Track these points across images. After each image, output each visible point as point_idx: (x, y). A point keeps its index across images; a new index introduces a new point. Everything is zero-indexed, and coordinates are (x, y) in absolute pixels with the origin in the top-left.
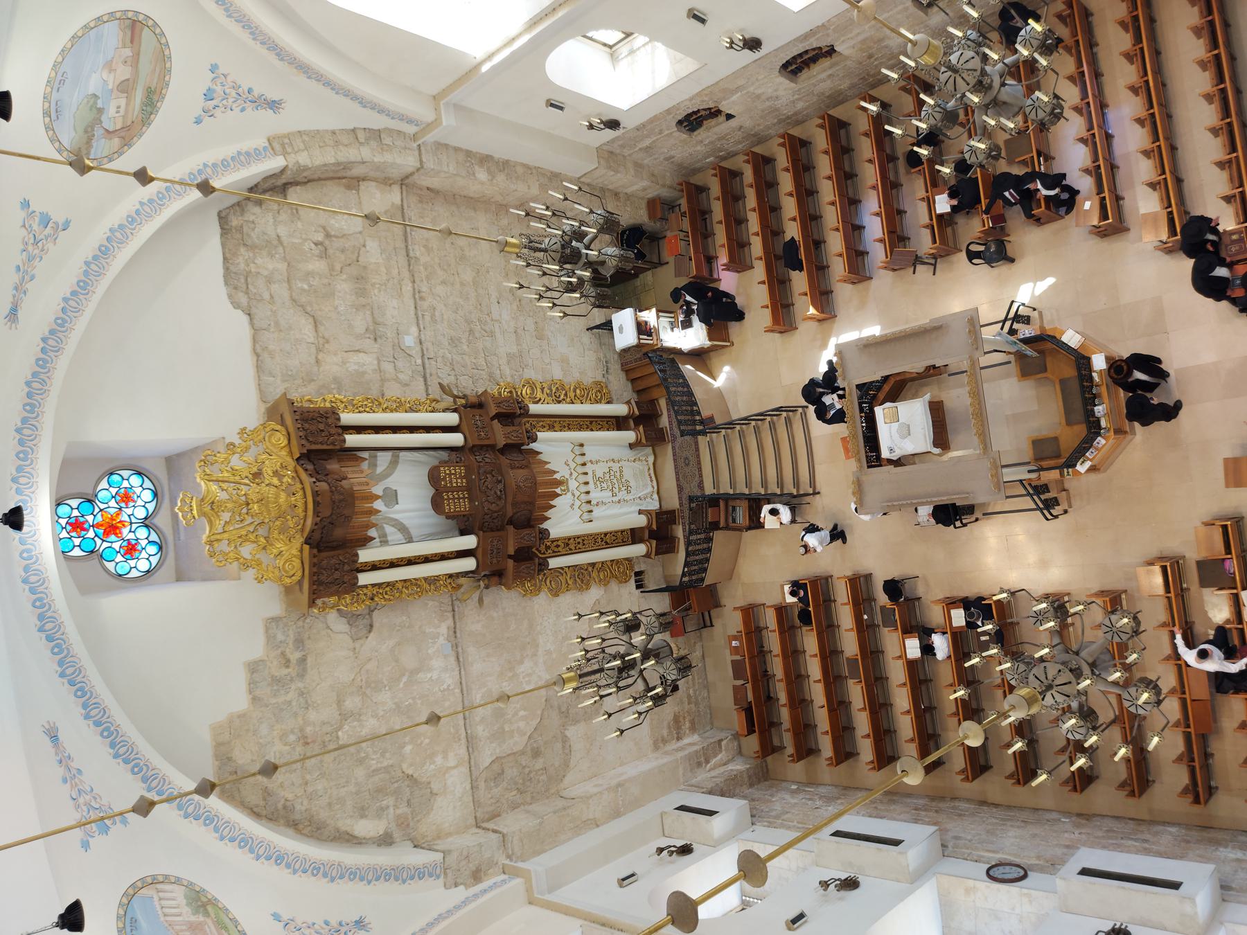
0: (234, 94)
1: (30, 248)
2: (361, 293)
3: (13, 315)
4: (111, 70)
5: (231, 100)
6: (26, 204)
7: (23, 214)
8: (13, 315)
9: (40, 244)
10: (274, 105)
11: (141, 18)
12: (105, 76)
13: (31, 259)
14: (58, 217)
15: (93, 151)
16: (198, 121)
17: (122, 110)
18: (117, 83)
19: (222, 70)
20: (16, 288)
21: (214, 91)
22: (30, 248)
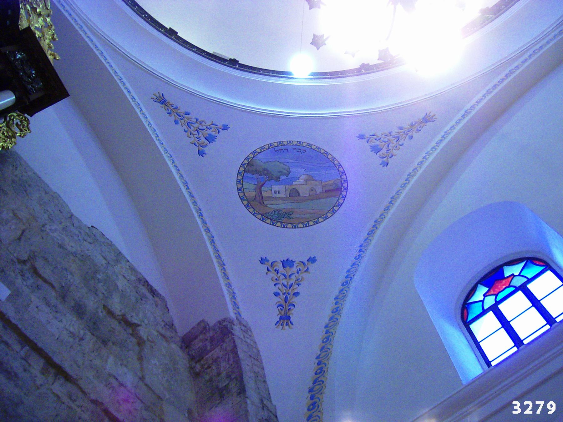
0: (289, 284)
1: (196, 125)
2: (79, 310)
3: (162, 101)
4: (306, 181)
5: (285, 282)
6: (225, 128)
7: (220, 125)
8: (162, 101)
9: (196, 133)
10: (285, 319)
11: (344, 193)
12: (303, 177)
13: (189, 124)
14: (210, 149)
15: (249, 175)
16: (263, 261)
17: (277, 195)
18: (297, 188)
19: (312, 267)
20: (176, 108)
21: (291, 266)
22: (196, 125)
